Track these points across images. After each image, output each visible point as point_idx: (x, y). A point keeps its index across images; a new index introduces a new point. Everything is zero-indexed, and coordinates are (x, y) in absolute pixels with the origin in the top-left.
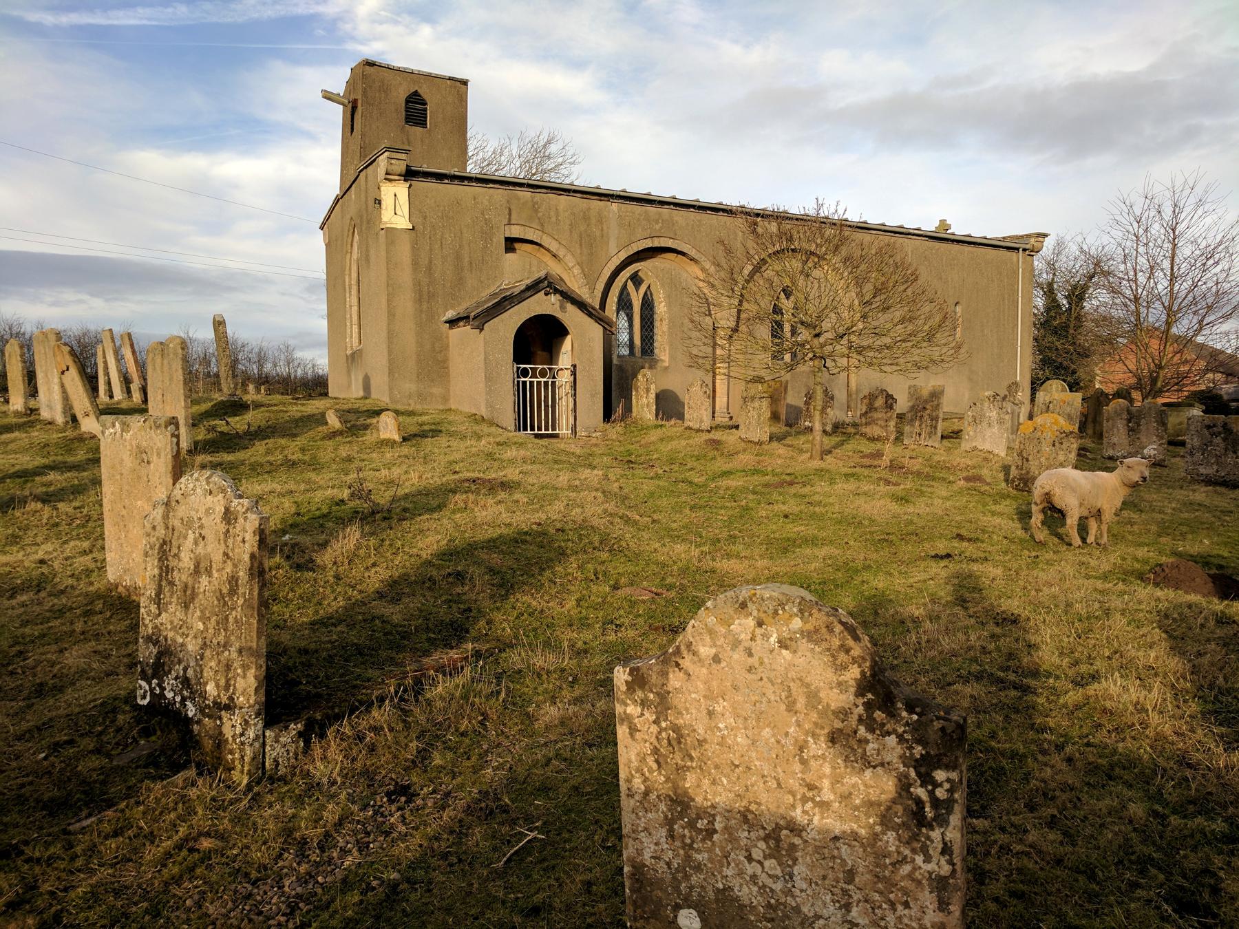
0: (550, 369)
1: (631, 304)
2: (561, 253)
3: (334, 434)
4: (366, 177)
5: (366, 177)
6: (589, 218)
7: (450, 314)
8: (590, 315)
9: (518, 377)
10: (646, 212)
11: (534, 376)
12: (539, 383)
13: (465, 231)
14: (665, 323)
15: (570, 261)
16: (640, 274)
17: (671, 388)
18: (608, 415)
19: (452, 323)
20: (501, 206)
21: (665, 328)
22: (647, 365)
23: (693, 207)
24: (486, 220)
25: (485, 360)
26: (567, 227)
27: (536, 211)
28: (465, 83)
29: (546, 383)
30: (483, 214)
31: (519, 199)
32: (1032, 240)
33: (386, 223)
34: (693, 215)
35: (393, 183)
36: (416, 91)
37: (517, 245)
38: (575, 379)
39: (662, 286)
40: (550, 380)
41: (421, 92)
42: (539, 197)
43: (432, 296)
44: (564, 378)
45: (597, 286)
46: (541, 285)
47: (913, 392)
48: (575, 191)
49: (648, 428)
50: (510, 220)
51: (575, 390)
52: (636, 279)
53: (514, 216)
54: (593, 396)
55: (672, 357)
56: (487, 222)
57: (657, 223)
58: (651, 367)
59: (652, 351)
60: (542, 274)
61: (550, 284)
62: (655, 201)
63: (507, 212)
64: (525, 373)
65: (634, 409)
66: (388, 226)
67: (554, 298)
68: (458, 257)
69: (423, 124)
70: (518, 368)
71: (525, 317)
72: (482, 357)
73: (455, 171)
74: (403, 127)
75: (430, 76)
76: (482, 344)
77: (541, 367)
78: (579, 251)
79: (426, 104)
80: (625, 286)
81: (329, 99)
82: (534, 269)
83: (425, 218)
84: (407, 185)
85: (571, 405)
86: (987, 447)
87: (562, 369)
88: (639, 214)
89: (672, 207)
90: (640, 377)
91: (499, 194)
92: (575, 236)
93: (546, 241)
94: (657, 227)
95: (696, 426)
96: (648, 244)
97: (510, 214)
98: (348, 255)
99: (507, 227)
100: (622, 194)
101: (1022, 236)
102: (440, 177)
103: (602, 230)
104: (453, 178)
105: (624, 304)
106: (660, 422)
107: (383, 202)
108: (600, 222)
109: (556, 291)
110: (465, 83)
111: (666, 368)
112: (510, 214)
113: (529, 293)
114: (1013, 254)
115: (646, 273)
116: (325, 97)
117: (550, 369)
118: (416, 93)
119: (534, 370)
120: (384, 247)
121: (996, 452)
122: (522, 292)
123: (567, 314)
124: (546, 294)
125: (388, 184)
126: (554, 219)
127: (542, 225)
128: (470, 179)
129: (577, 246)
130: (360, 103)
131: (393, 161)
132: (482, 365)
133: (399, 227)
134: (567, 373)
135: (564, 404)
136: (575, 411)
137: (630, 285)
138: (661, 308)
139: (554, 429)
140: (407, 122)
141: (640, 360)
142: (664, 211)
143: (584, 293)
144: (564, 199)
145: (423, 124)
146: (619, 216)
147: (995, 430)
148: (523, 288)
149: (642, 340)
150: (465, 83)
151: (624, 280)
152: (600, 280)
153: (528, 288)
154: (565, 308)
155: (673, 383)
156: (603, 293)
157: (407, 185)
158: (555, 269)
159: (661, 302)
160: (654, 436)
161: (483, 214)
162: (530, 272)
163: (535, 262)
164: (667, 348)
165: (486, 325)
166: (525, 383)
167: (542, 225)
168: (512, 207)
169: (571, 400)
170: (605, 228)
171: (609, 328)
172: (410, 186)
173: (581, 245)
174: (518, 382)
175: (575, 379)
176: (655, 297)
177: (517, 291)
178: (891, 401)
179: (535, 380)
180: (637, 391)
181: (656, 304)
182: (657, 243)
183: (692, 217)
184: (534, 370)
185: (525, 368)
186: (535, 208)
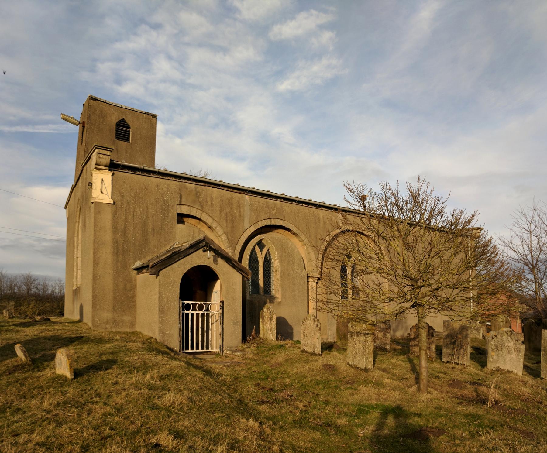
0: (205, 304)
1: (257, 261)
2: (214, 225)
3: (21, 367)
4: (86, 170)
5: (86, 170)
6: (232, 204)
8: (234, 266)
9: (183, 310)
10: (267, 202)
11: (194, 309)
12: (198, 314)
13: (150, 207)
14: (279, 273)
15: (220, 231)
16: (263, 241)
17: (282, 316)
18: (244, 339)
20: (175, 192)
21: (279, 276)
22: (268, 301)
23: (295, 201)
24: (164, 200)
25: (159, 297)
26: (218, 209)
27: (198, 197)
28: (155, 117)
29: (203, 314)
30: (162, 197)
31: (187, 189)
33: (95, 199)
34: (295, 206)
35: (101, 172)
37: (186, 219)
38: (223, 311)
39: (277, 249)
40: (206, 313)
42: (200, 188)
44: (215, 311)
45: (237, 248)
46: (201, 245)
47: (446, 325)
48: (224, 186)
49: (272, 348)
50: (181, 201)
51: (223, 319)
52: (260, 244)
53: (184, 199)
54: (235, 324)
55: (283, 296)
56: (165, 202)
57: (273, 210)
58: (270, 302)
59: (270, 291)
60: (201, 237)
62: (272, 196)
63: (179, 196)
64: (188, 307)
65: (261, 332)
66: (96, 201)
67: (209, 254)
68: (145, 224)
70: (183, 304)
71: (189, 267)
72: (157, 295)
73: (145, 167)
74: (114, 141)
76: (158, 287)
77: (199, 303)
78: (225, 225)
80: (254, 249)
81: (66, 120)
82: (196, 235)
83: (123, 197)
84: (111, 173)
85: (220, 331)
86: (507, 367)
87: (213, 304)
88: (263, 204)
89: (282, 200)
90: (265, 310)
91: (174, 184)
92: (223, 215)
93: (204, 217)
94: (274, 212)
95: (311, 350)
96: (268, 222)
97: (181, 198)
99: (178, 207)
100: (252, 190)
102: (134, 170)
103: (240, 212)
104: (143, 171)
105: (253, 260)
106: (282, 343)
107: (93, 185)
108: (239, 207)
109: (211, 249)
111: (280, 303)
112: (181, 198)
113: (192, 250)
115: (267, 241)
116: (63, 119)
117: (205, 304)
119: (194, 305)
120: (93, 216)
121: (516, 372)
122: (187, 249)
123: (218, 266)
124: (204, 251)
126: (209, 203)
127: (202, 206)
128: (155, 173)
129: (224, 221)
130: (86, 123)
132: (157, 301)
133: (104, 202)
134: (217, 307)
135: (215, 329)
136: (223, 335)
137: (257, 247)
138: (276, 264)
139: (207, 348)
141: (264, 297)
142: (278, 203)
143: (229, 251)
144: (216, 191)
146: (251, 204)
147: (514, 355)
148: (188, 246)
149: (265, 284)
151: (253, 245)
152: (239, 244)
153: (192, 246)
154: (217, 261)
155: (285, 313)
156: (240, 253)
157: (111, 173)
158: (211, 236)
159: (276, 260)
160: (280, 357)
161: (162, 197)
162: (193, 237)
163: (197, 230)
164: (280, 290)
165: (161, 272)
166: (187, 314)
167: (202, 206)
168: (182, 193)
169: (220, 327)
170: (242, 210)
171: (246, 276)
172: (113, 174)
173: (227, 221)
174: (183, 314)
175: (223, 311)
176: (272, 256)
177: (183, 248)
178: (432, 331)
179: (195, 312)
180: (263, 319)
181: (273, 261)
182: (274, 222)
183: (294, 208)
184: (194, 305)
185: (188, 304)
186: (197, 195)
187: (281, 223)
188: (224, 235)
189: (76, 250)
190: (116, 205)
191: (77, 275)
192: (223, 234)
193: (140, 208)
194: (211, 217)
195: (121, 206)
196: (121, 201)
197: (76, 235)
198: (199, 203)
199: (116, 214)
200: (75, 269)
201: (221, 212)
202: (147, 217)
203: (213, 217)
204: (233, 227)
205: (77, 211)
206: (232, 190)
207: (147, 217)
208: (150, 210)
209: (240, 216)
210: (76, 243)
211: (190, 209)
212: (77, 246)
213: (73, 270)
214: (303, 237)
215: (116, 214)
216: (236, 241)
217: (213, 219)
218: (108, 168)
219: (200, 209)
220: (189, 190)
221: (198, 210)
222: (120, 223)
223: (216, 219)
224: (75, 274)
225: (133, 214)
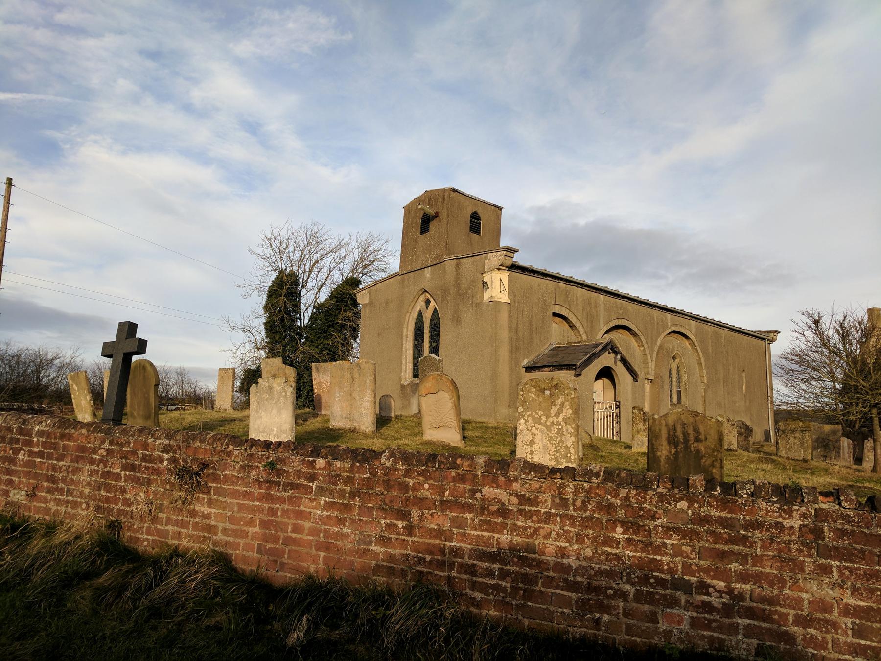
2: (577, 325)
7: (525, 362)
10: (616, 302)
13: (534, 307)
19: (529, 369)
20: (552, 291)
27: (567, 297)
31: (560, 288)
32: (772, 335)
33: (494, 298)
35: (501, 272)
36: (476, 211)
41: (478, 212)
43: (518, 349)
56: (545, 301)
61: (612, 348)
66: (496, 300)
68: (531, 323)
69: (478, 232)
75: (484, 202)
78: (586, 324)
79: (480, 220)
83: (515, 296)
89: (627, 300)
91: (551, 284)
97: (556, 298)
98: (408, 314)
101: (764, 332)
110: (500, 208)
112: (556, 298)
114: (762, 343)
118: (475, 213)
125: (497, 272)
126: (575, 303)
127: (570, 305)
131: (507, 258)
140: (471, 230)
144: (580, 291)
145: (478, 232)
146: (604, 304)
150: (500, 208)
167: (570, 305)
187: (626, 323)
189: (404, 342)
191: (406, 368)
197: (405, 326)
198: (567, 303)
200: (404, 362)
202: (532, 316)
204: (592, 327)
205: (412, 302)
206: (591, 289)
207: (532, 316)
208: (534, 309)
209: (597, 316)
210: (405, 334)
212: (407, 337)
213: (401, 363)
214: (642, 338)
217: (577, 318)
218: (507, 269)
220: (561, 289)
224: (404, 368)
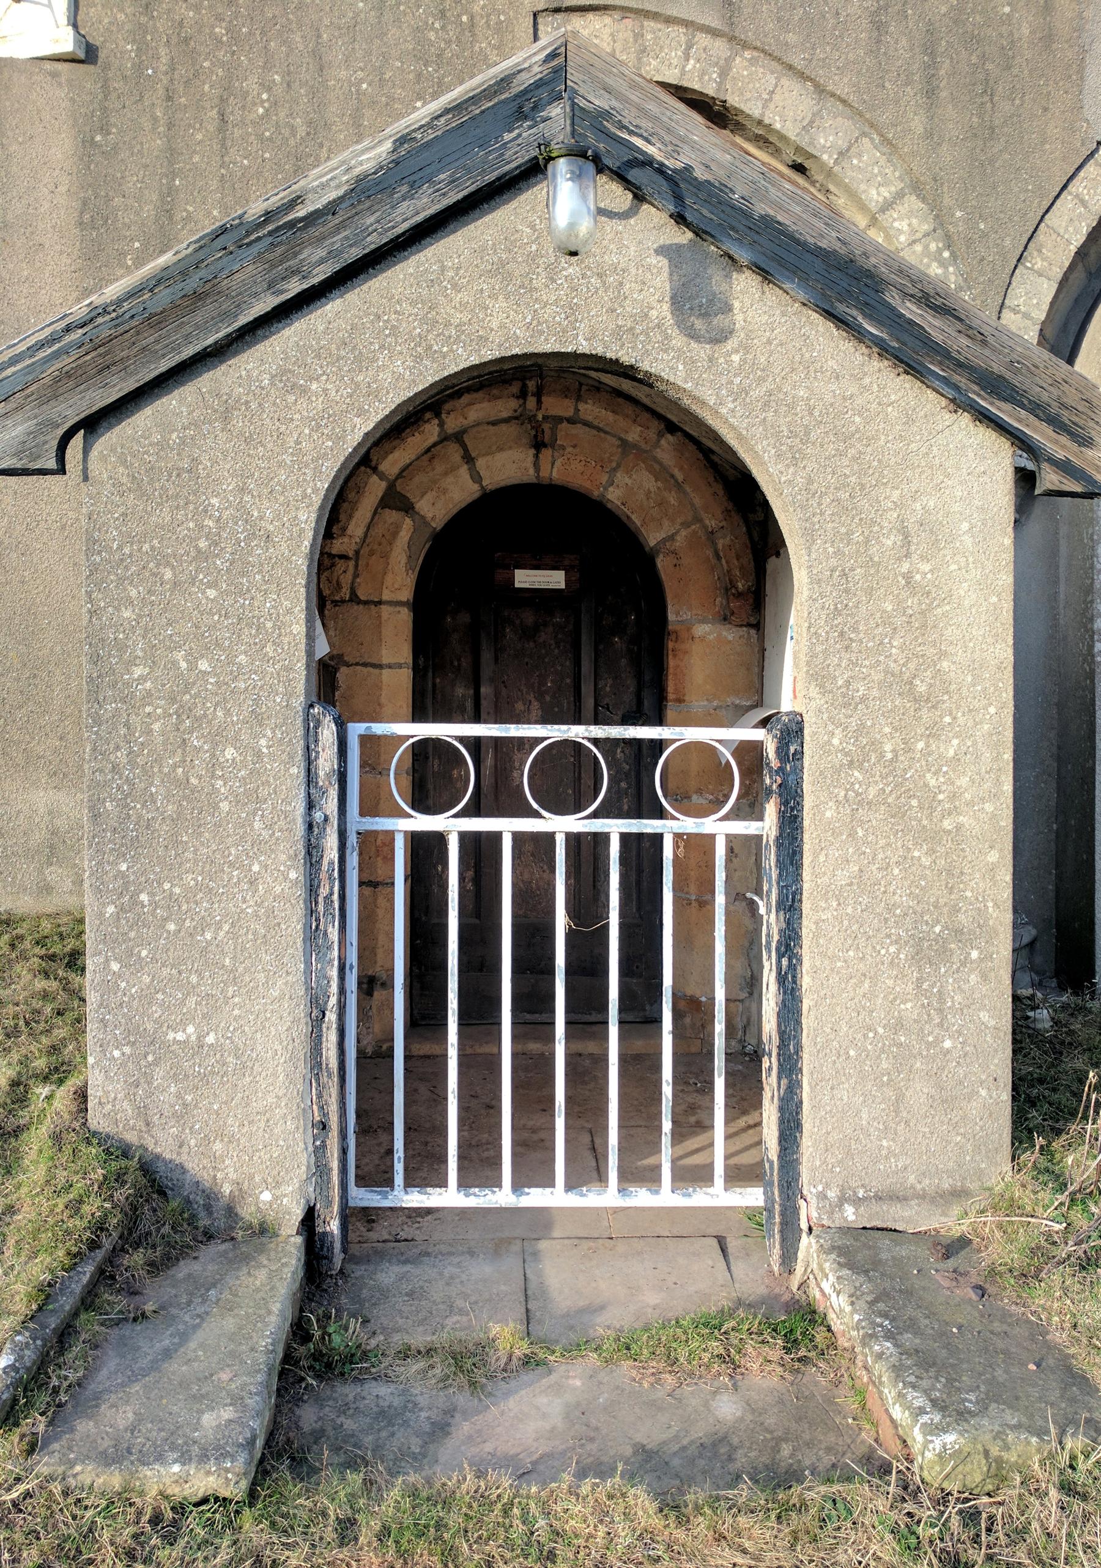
78: (918, 124)
152: (1034, 261)
173: (931, 93)
188: (912, 202)
190: (107, 67)
192: (900, 195)
193: (267, 66)
194: (803, 76)
195: (139, 68)
196: (139, 34)
199: (104, 130)
201: (879, 27)
203: (820, 74)
209: (1048, 39)
211: (638, 36)
215: (104, 130)
216: (1012, 244)
217: (820, 90)
219: (715, 23)
221: (703, 40)
222: (131, 184)
223: (841, 86)
225: (222, 115)
